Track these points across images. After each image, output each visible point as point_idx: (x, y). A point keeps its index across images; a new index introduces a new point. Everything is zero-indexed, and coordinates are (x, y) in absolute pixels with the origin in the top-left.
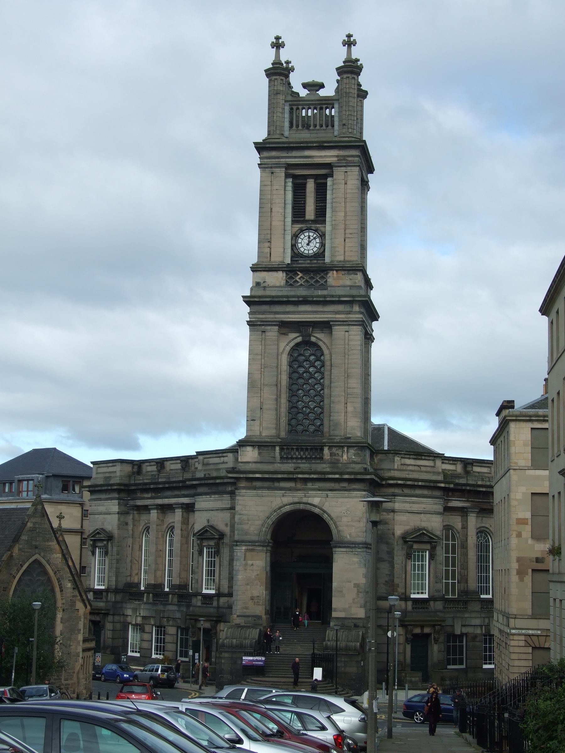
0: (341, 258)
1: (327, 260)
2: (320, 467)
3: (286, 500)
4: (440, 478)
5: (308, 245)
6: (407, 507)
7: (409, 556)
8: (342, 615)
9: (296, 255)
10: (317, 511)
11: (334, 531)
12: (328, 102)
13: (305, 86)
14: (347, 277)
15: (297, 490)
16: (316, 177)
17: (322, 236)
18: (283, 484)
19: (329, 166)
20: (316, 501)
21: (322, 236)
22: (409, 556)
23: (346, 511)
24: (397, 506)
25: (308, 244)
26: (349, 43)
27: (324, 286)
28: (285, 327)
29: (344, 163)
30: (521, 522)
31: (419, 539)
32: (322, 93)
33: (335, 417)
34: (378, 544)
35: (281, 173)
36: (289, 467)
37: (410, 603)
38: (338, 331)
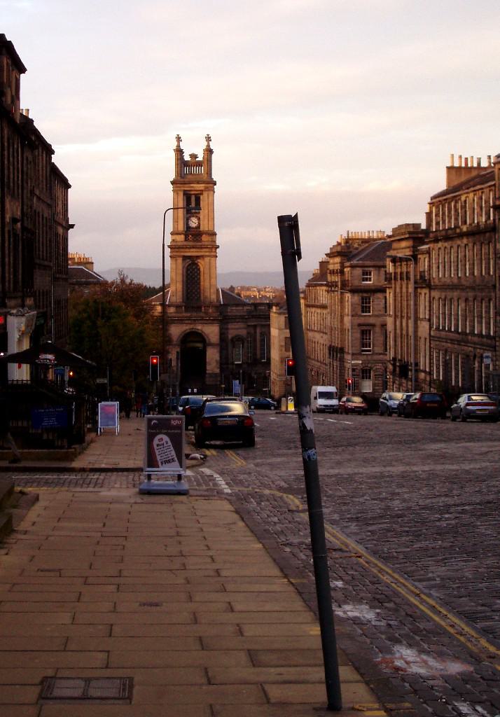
0: (207, 229)
1: (201, 229)
2: (202, 314)
3: (187, 328)
4: (245, 314)
5: (193, 222)
6: (233, 327)
7: (234, 347)
8: (210, 372)
9: (188, 227)
10: (200, 332)
11: (207, 339)
12: (199, 164)
14: (210, 237)
15: (191, 324)
17: (199, 219)
18: (187, 322)
20: (199, 328)
21: (199, 219)
22: (234, 347)
23: (212, 332)
24: (229, 327)
26: (208, 139)
27: (201, 241)
29: (207, 189)
30: (281, 346)
31: (238, 339)
32: (197, 159)
33: (206, 294)
34: (224, 343)
36: (189, 314)
37: (234, 366)
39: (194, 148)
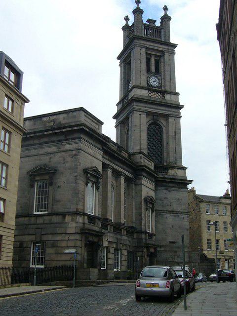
13: (149, 21)
16: (156, 56)
19: (163, 52)
25: (154, 82)
26: (166, 9)
28: (148, 114)
35: (143, 51)
38: (171, 120)
39: (153, 14)
